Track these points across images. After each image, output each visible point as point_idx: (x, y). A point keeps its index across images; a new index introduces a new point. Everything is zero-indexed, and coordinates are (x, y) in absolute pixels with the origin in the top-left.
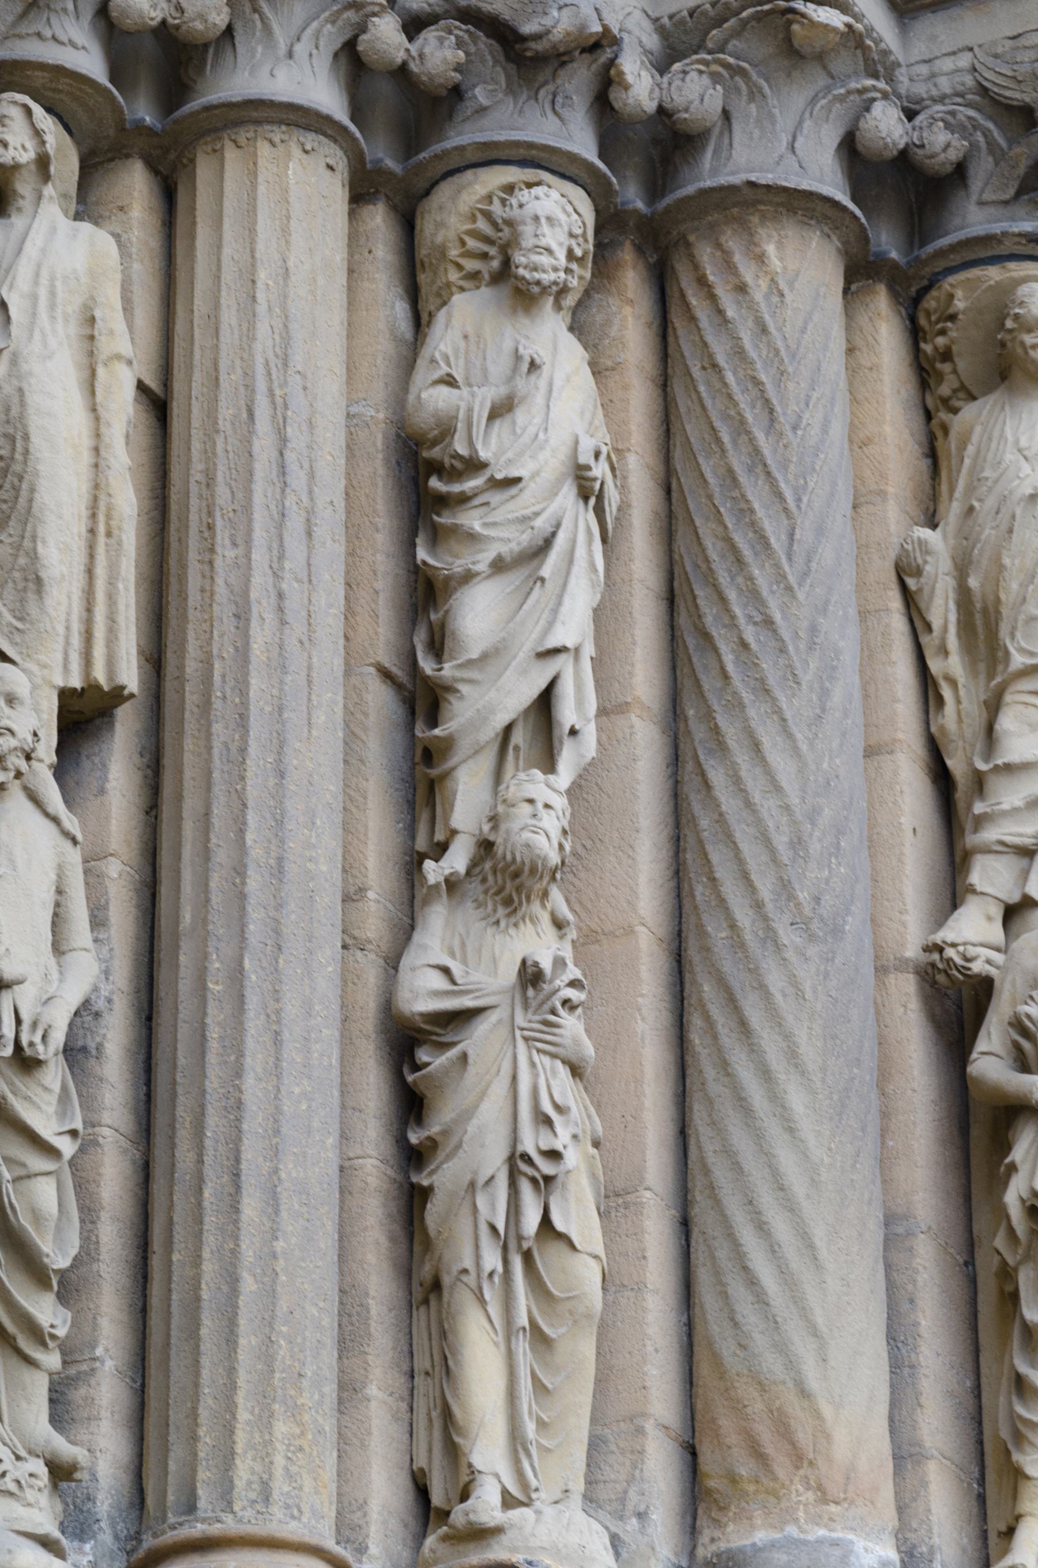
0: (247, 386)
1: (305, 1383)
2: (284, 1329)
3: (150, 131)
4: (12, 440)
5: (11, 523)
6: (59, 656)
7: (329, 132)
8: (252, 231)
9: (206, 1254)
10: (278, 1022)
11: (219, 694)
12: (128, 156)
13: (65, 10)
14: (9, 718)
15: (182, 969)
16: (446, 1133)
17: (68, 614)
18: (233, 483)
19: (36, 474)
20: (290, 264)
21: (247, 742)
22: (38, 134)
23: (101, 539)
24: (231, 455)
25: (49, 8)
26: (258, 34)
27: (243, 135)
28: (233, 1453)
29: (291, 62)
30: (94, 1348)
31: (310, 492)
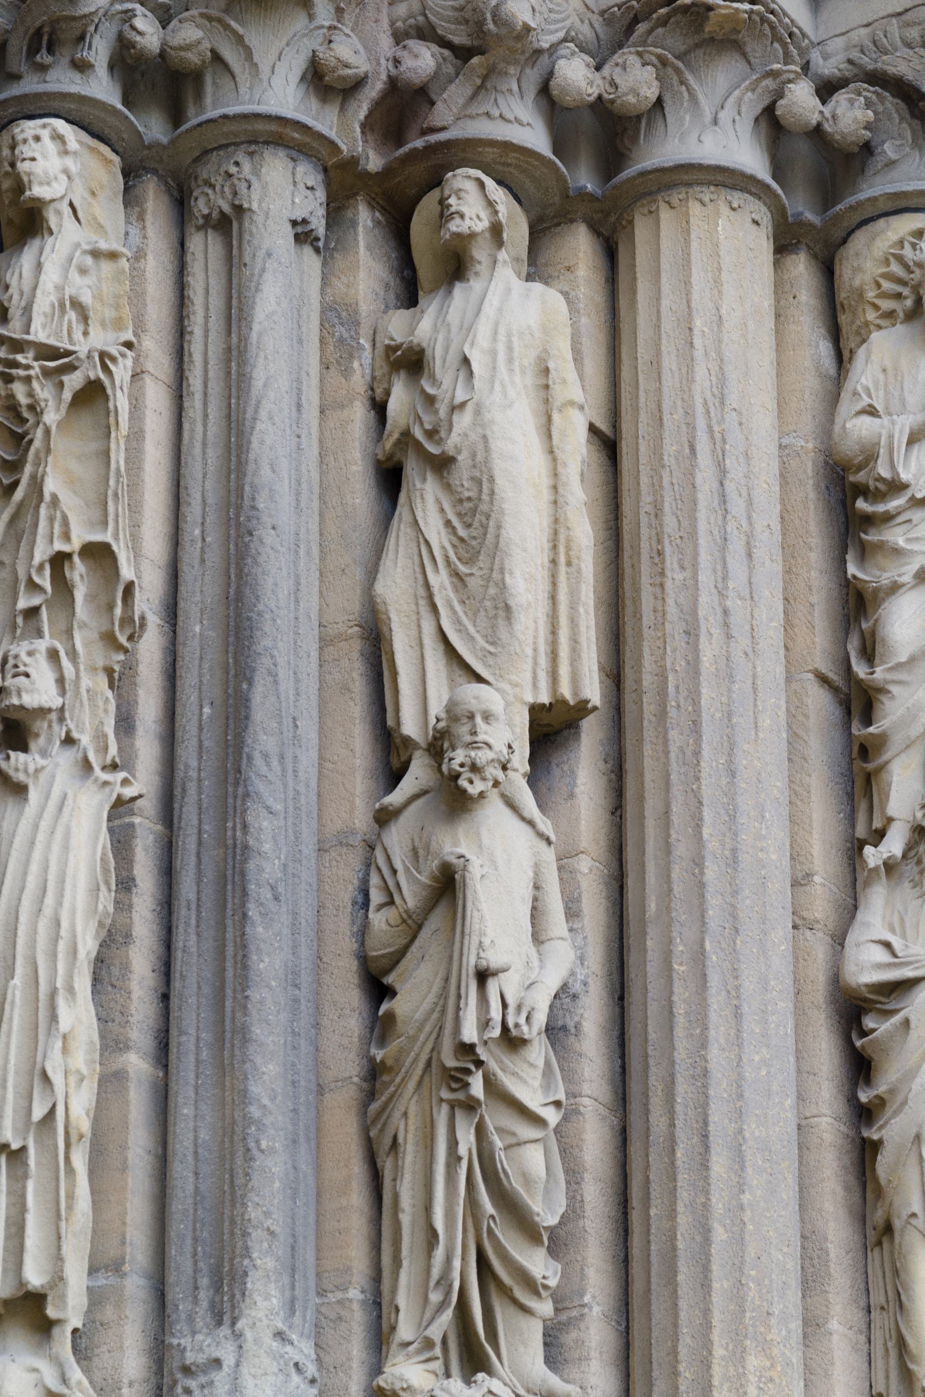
0: (688, 424)
1: (773, 1321)
2: (753, 1273)
3: (591, 197)
4: (479, 482)
5: (481, 558)
6: (528, 676)
7: (753, 190)
8: (687, 283)
9: (680, 1208)
10: (738, 997)
11: (673, 703)
12: (572, 221)
13: (510, 91)
14: (486, 733)
15: (649, 953)
16: (892, 1091)
17: (535, 637)
18: (679, 513)
19: (502, 512)
20: (723, 311)
21: (700, 746)
22: (491, 204)
23: (563, 568)
24: (676, 487)
25: (495, 88)
28: (710, 1386)
29: (717, 128)
30: (582, 1296)
31: (749, 518)
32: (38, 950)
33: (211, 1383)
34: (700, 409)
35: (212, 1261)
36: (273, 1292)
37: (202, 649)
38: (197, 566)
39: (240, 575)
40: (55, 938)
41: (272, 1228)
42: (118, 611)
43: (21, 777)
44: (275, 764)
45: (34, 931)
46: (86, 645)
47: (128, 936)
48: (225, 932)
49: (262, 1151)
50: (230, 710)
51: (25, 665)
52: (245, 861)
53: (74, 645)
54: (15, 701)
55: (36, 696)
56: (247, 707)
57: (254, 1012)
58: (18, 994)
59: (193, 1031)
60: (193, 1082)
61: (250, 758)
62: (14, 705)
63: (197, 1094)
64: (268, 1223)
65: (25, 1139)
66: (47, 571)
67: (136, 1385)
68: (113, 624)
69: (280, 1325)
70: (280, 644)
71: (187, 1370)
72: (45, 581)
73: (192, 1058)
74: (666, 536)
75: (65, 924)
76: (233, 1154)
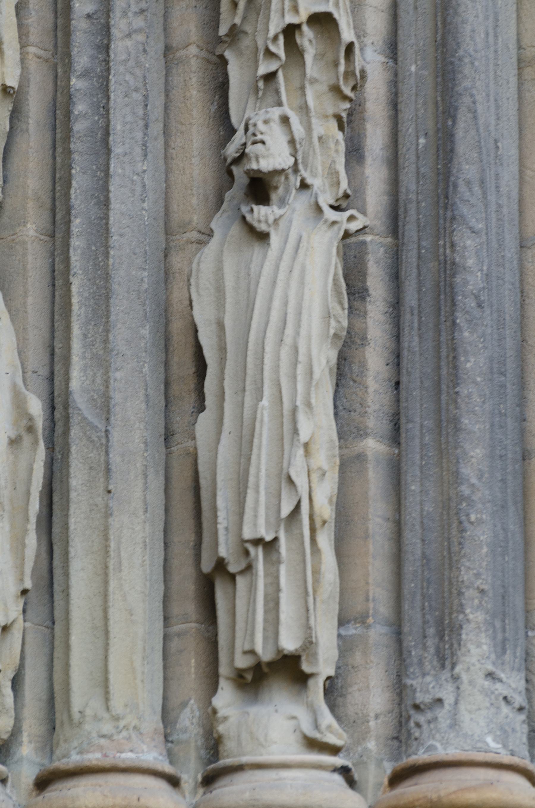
32: (281, 373)
33: (435, 719)
35: (437, 613)
36: (484, 641)
37: (417, 87)
38: (411, 13)
39: (444, 22)
40: (295, 363)
41: (482, 587)
42: (342, 68)
43: (263, 227)
44: (476, 189)
45: (277, 358)
46: (318, 97)
47: (364, 338)
48: (439, 335)
49: (472, 523)
50: (440, 142)
51: (262, 133)
52: (453, 275)
53: (306, 102)
54: (254, 166)
55: (271, 160)
56: (452, 142)
57: (463, 406)
58: (266, 414)
59: (417, 419)
60: (418, 462)
61: (455, 186)
62: (253, 170)
63: (422, 472)
64: (478, 583)
65: (277, 532)
66: (281, 40)
67: (382, 716)
68: (338, 79)
69: (490, 667)
70: (478, 83)
71: (417, 707)
72: (279, 49)
73: (417, 442)
75: (302, 350)
76: (450, 525)
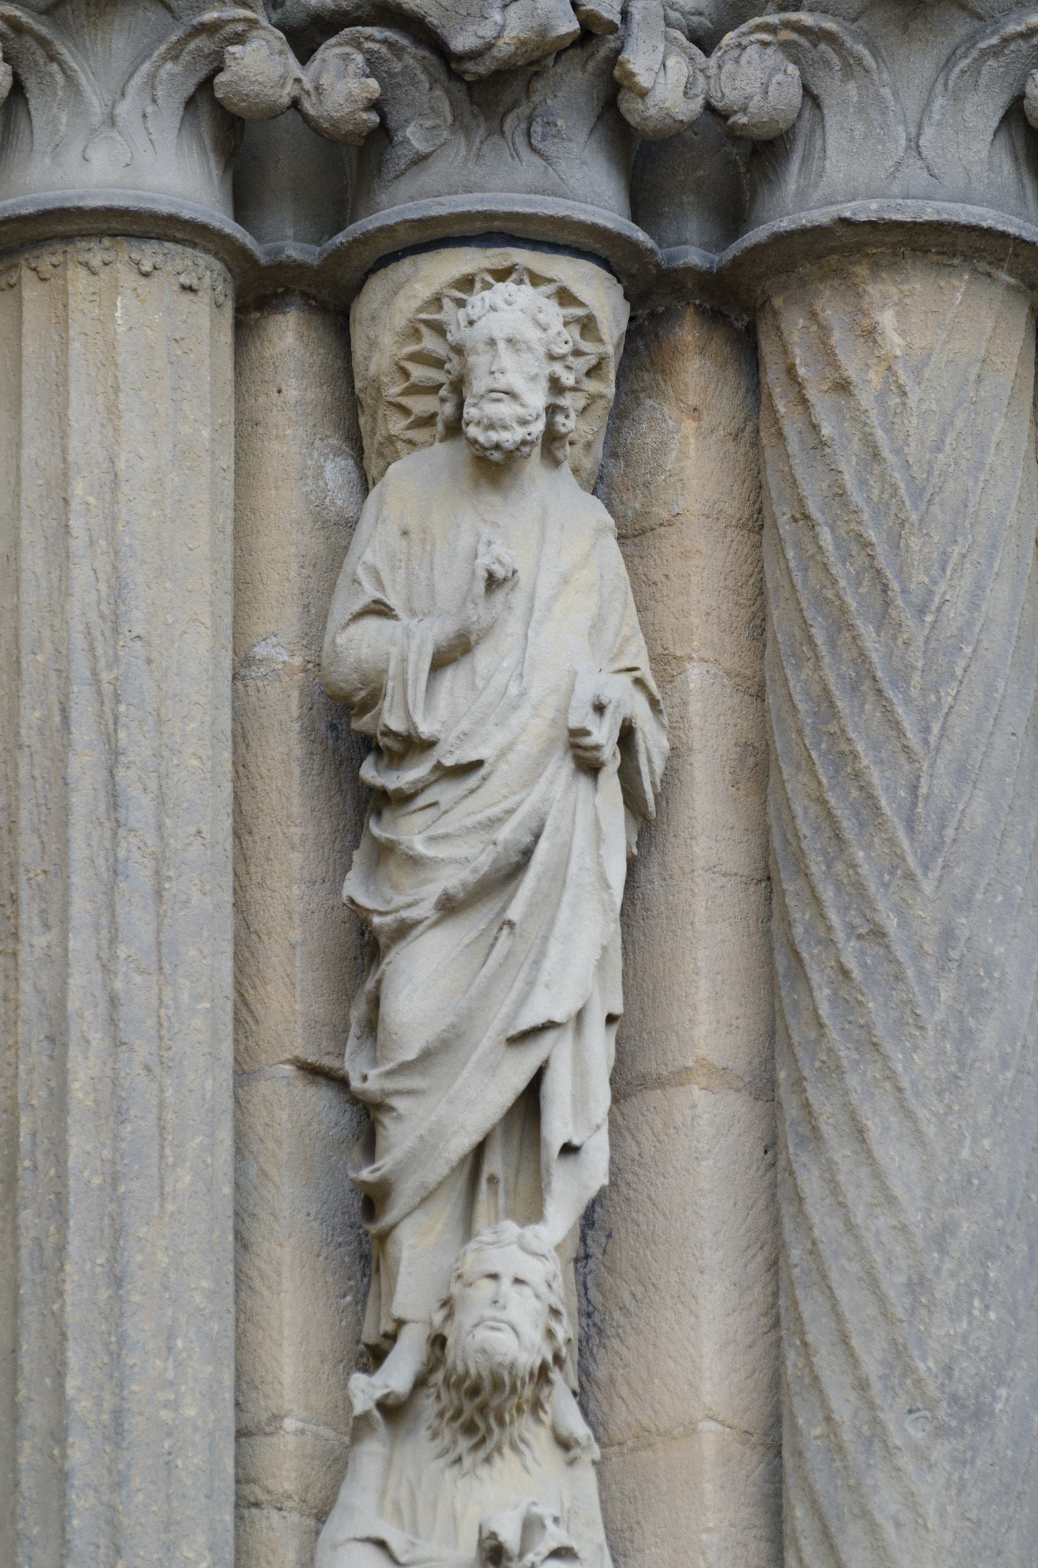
7: (179, 236)
8: (63, 417)
18: (43, 827)
20: (121, 465)
24: (39, 783)
26: (60, 93)
27: (46, 261)
29: (115, 134)
31: (160, 827)
34: (79, 642)
74: (22, 870)
